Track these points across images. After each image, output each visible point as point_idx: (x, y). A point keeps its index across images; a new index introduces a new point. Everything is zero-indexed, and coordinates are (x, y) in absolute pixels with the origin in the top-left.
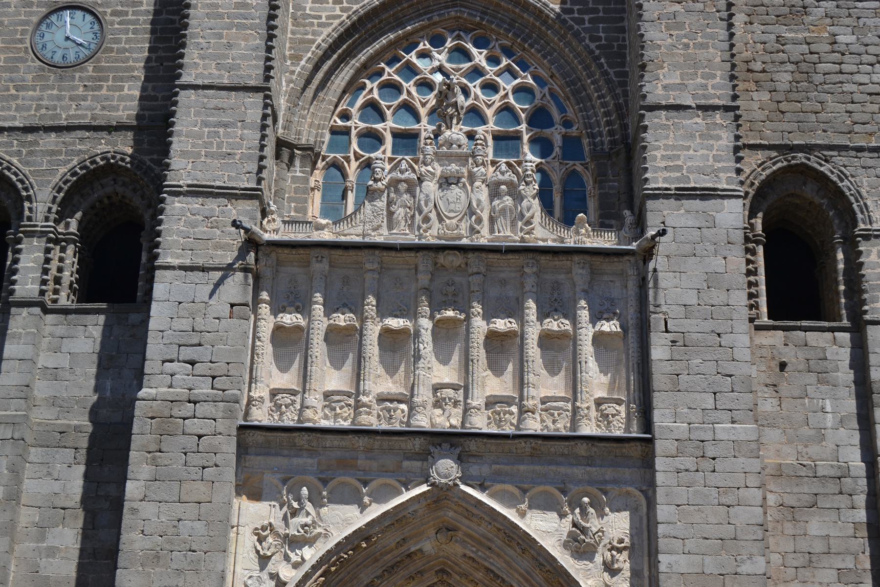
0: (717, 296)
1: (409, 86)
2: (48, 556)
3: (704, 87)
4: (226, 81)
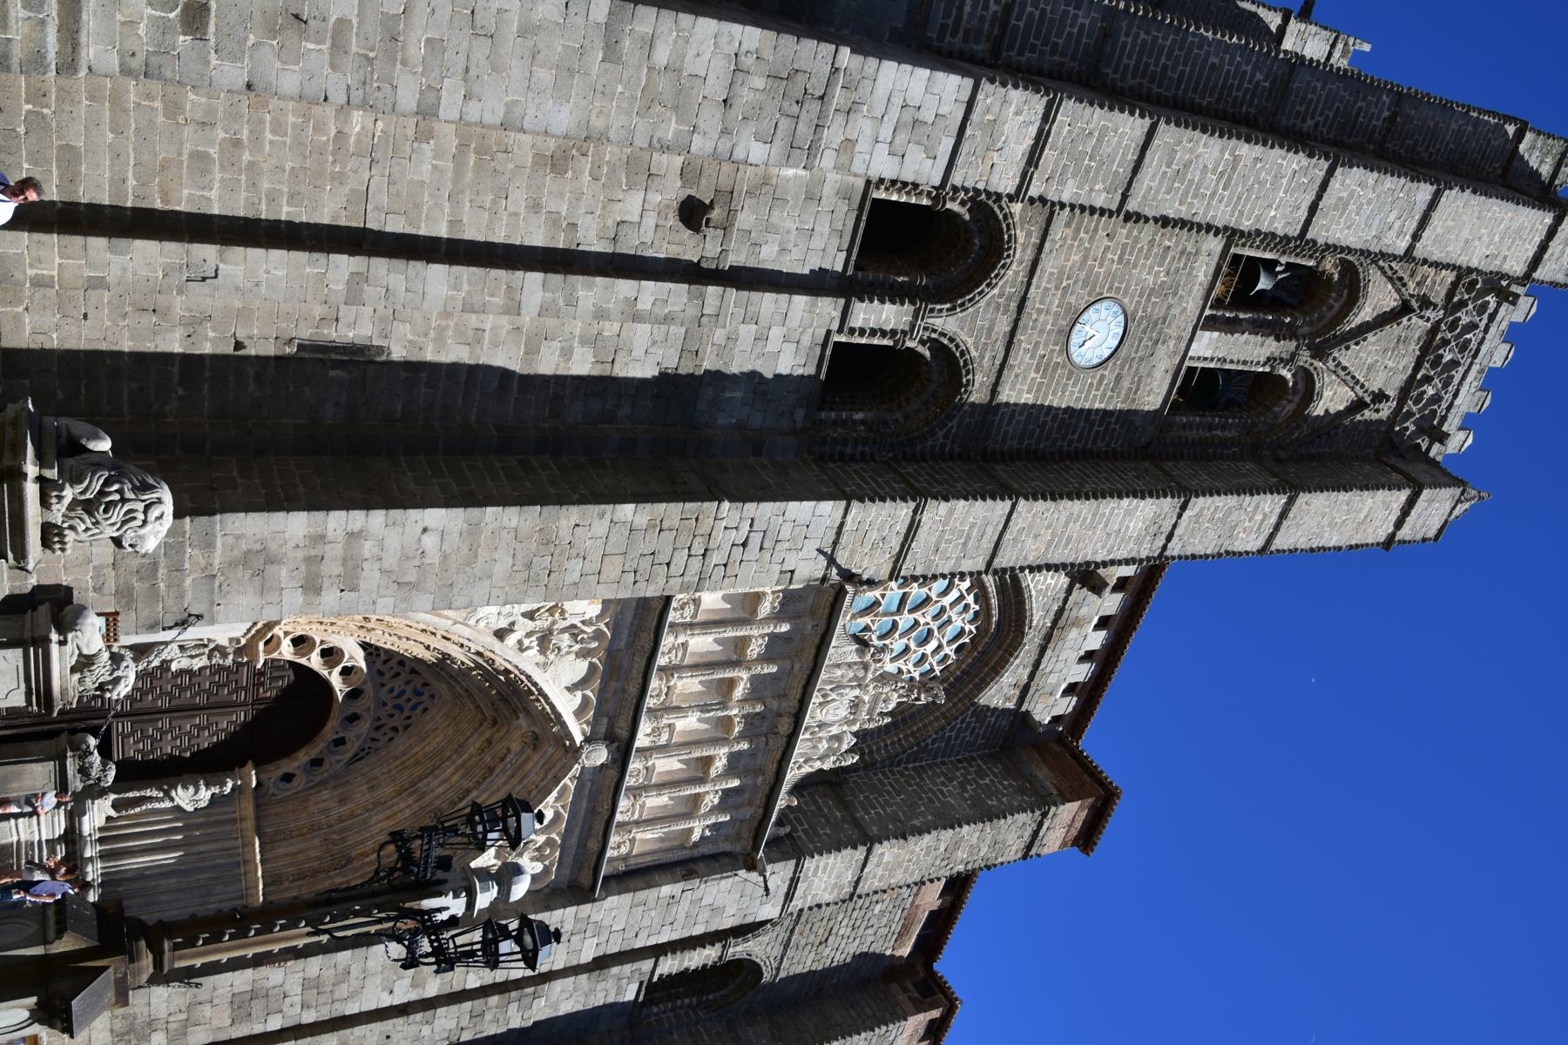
2: (562, 349)
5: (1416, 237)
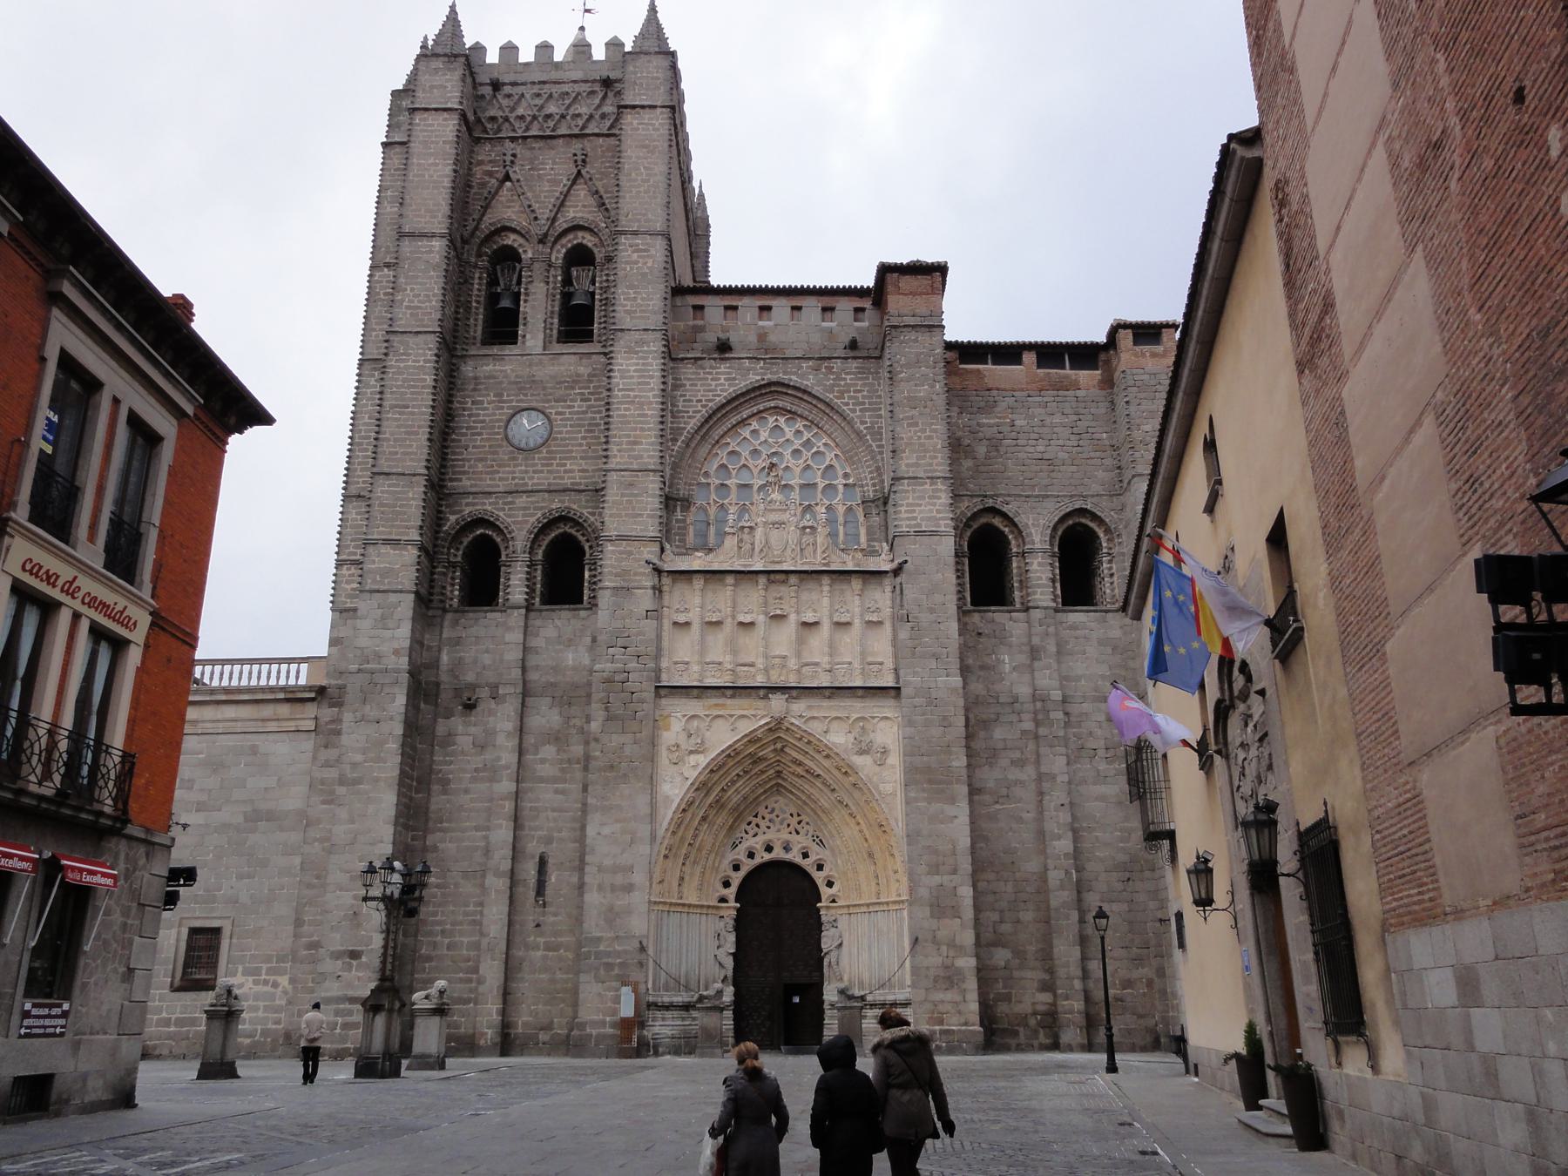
0: (938, 598)
1: (745, 453)
3: (931, 465)
4: (635, 467)
5: (433, 235)
